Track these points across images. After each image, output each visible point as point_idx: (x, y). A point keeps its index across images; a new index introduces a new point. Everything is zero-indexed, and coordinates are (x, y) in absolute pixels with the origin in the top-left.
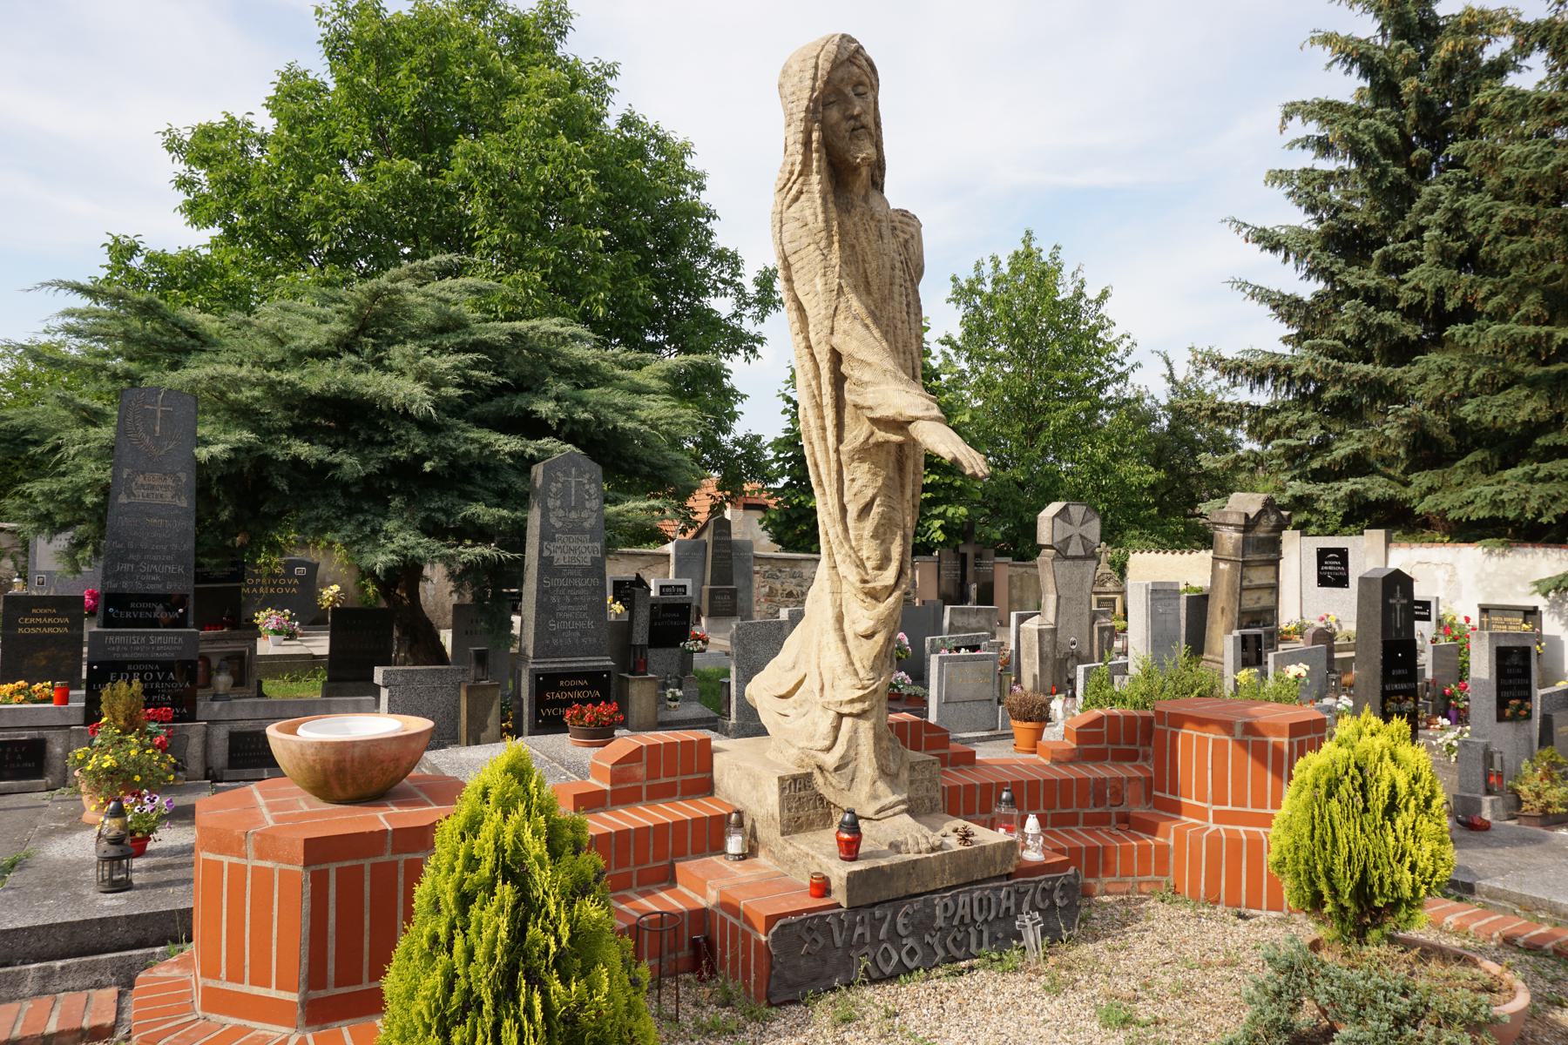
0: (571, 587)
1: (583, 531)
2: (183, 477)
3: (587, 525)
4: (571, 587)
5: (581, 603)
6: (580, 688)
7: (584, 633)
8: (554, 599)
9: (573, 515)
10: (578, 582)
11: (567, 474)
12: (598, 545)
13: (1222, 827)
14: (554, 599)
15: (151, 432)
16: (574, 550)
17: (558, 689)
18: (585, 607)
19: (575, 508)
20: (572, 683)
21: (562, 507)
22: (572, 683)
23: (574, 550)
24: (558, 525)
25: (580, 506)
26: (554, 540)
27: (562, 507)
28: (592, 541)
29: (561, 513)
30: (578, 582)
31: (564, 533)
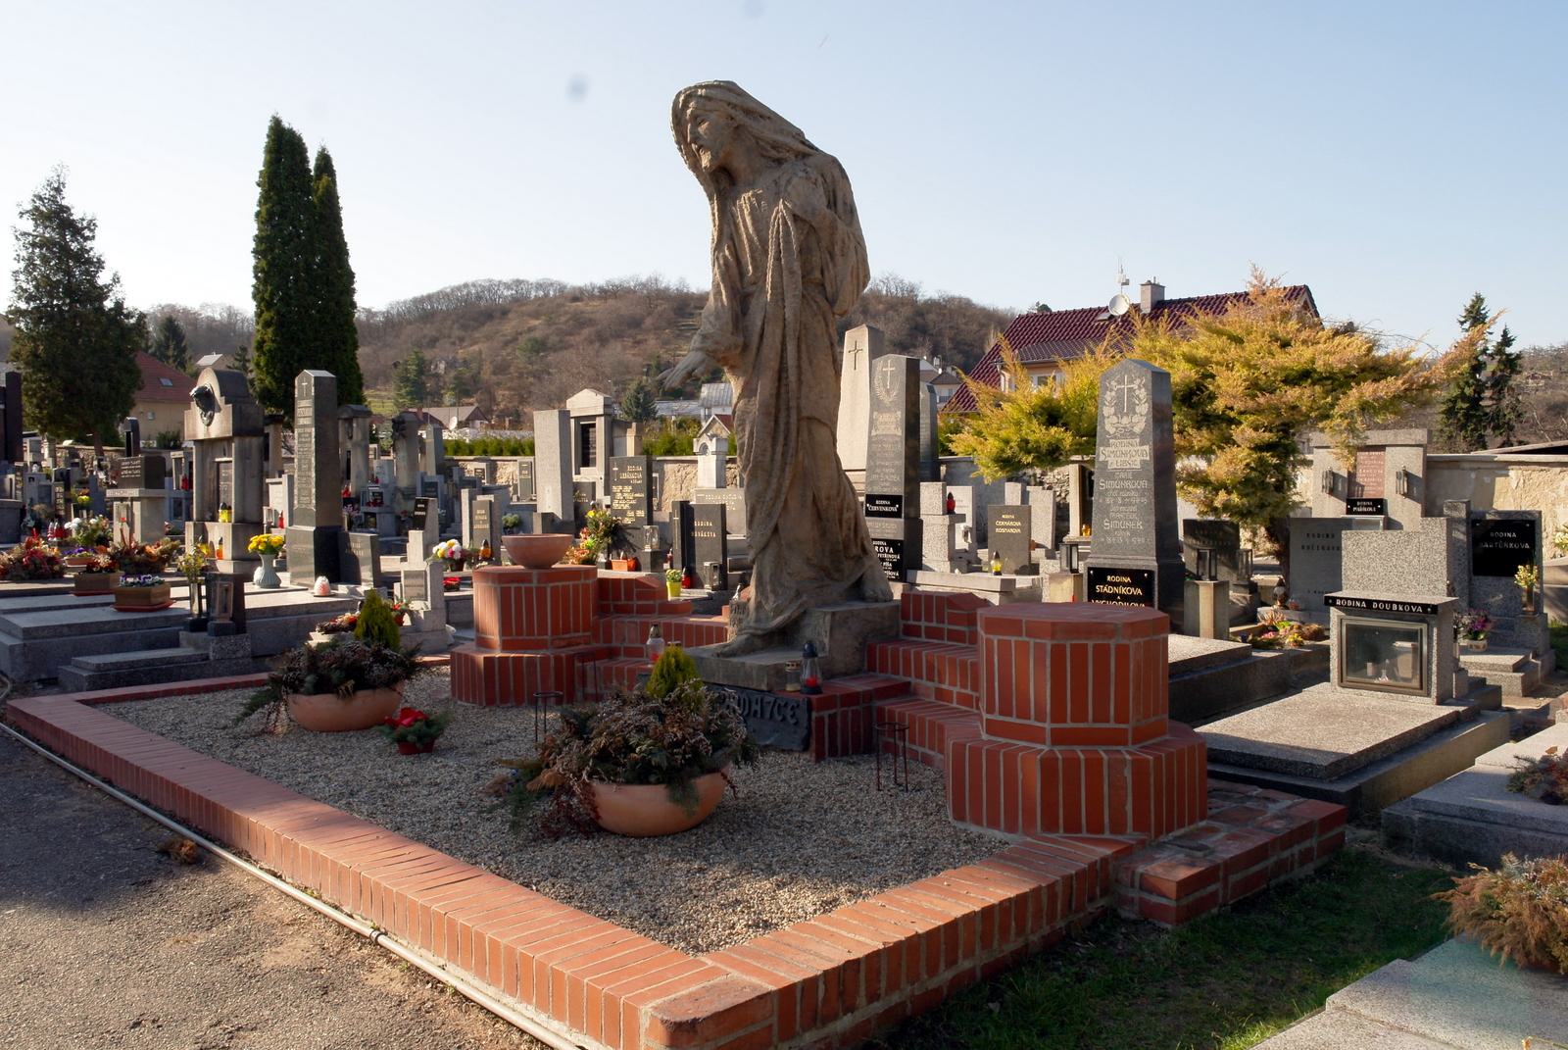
0: (1122, 490)
1: (1133, 434)
2: (899, 413)
3: (1137, 430)
4: (1122, 490)
5: (1130, 504)
6: (1125, 585)
7: (1134, 533)
8: (1108, 501)
9: (1125, 420)
10: (1127, 484)
11: (1120, 382)
12: (1147, 448)
13: (1056, 749)
14: (1108, 501)
15: (885, 386)
16: (1125, 454)
17: (1104, 582)
18: (1134, 509)
19: (1127, 414)
20: (1117, 579)
21: (1115, 414)
22: (1117, 579)
23: (1125, 454)
24: (1112, 431)
25: (1132, 411)
26: (1109, 445)
27: (1115, 414)
28: (1142, 443)
29: (1115, 419)
30: (1127, 484)
31: (1115, 438)
